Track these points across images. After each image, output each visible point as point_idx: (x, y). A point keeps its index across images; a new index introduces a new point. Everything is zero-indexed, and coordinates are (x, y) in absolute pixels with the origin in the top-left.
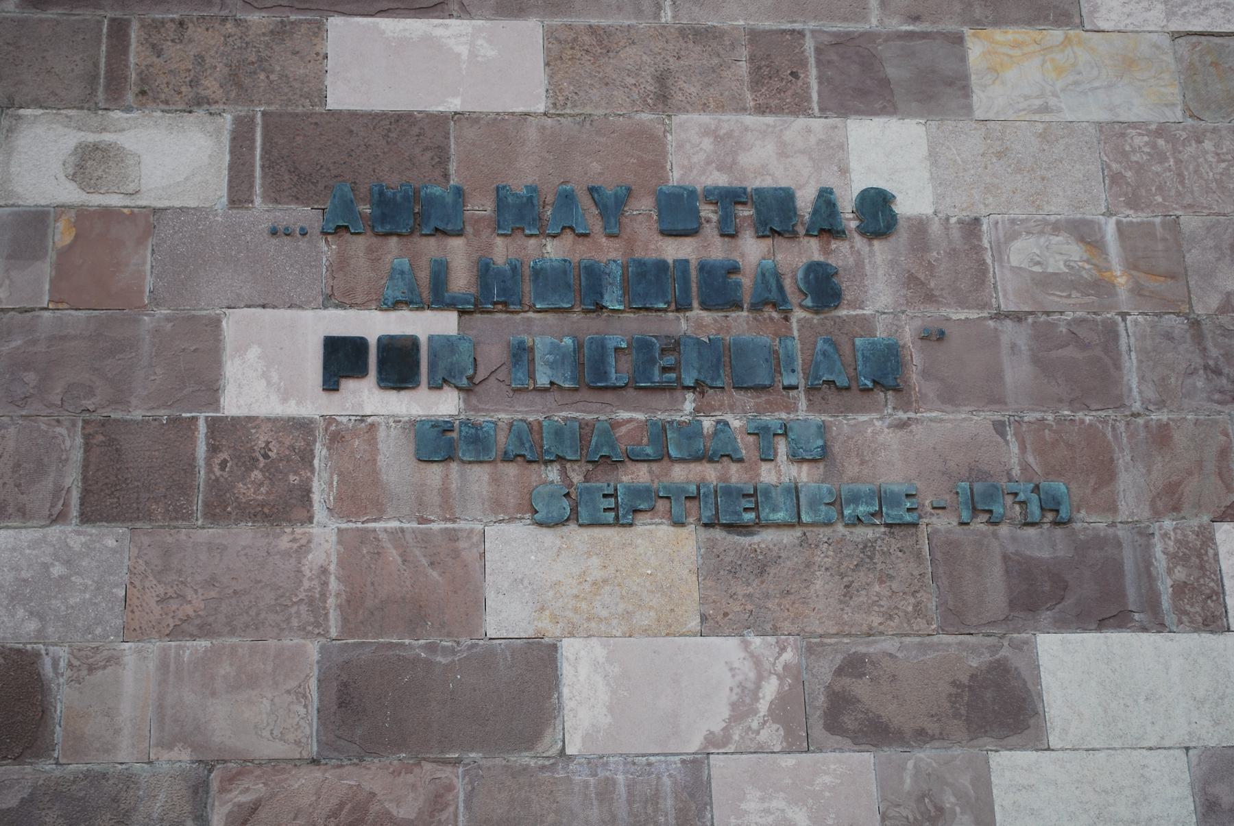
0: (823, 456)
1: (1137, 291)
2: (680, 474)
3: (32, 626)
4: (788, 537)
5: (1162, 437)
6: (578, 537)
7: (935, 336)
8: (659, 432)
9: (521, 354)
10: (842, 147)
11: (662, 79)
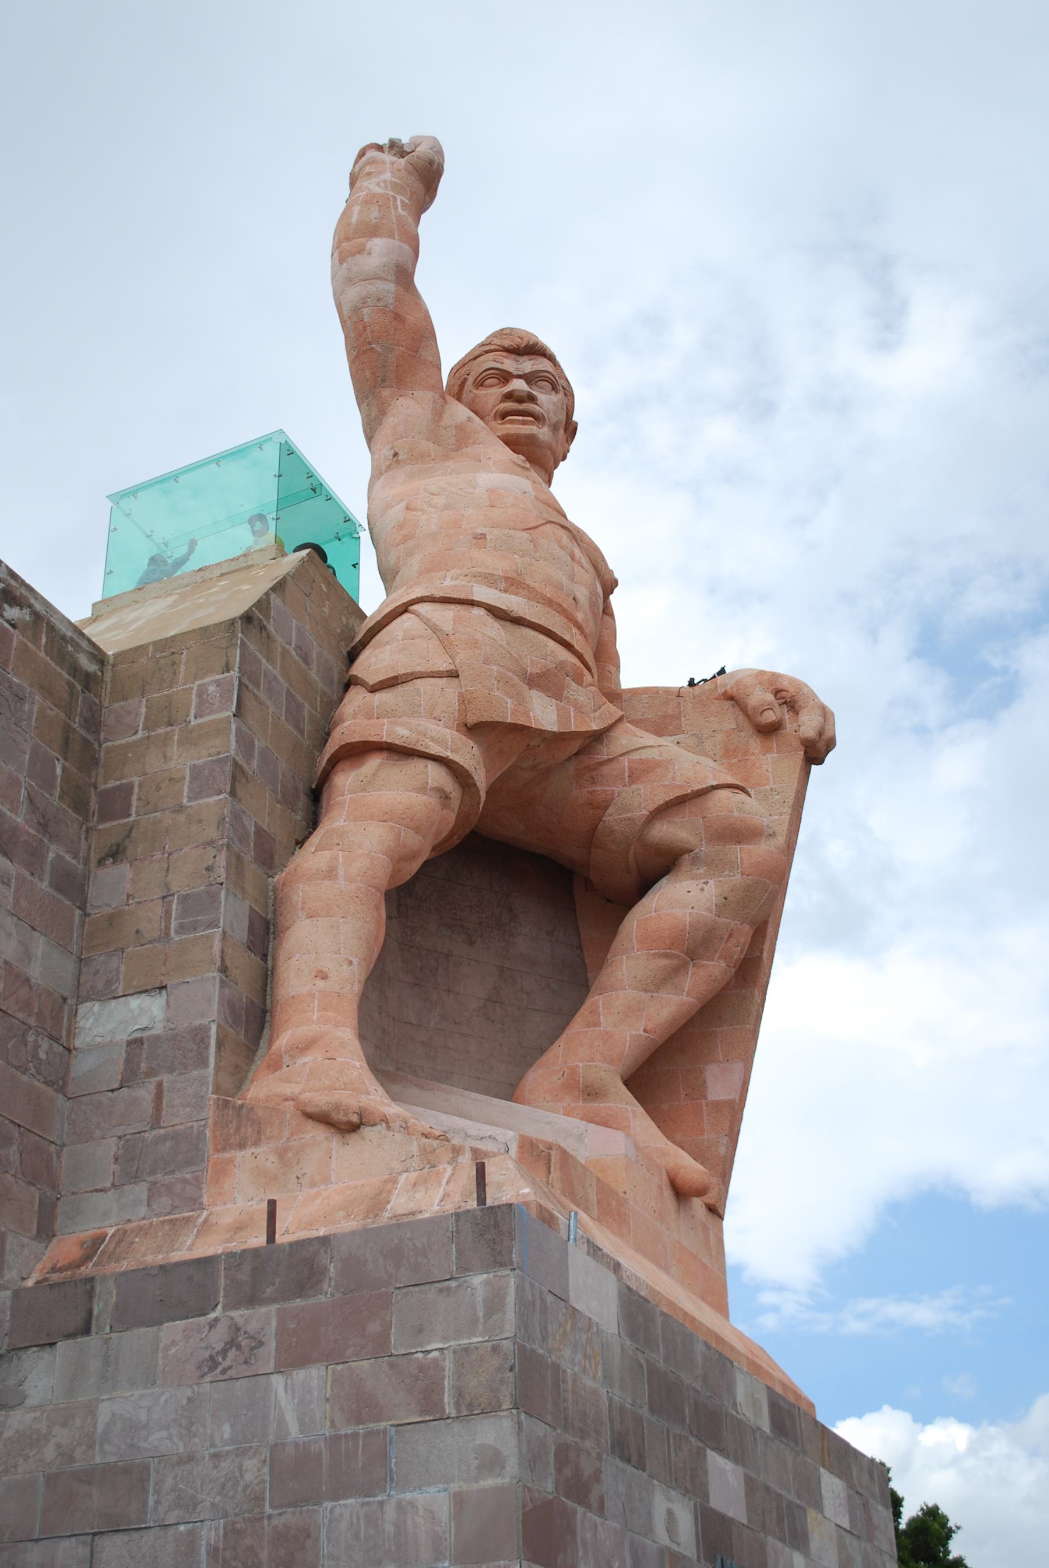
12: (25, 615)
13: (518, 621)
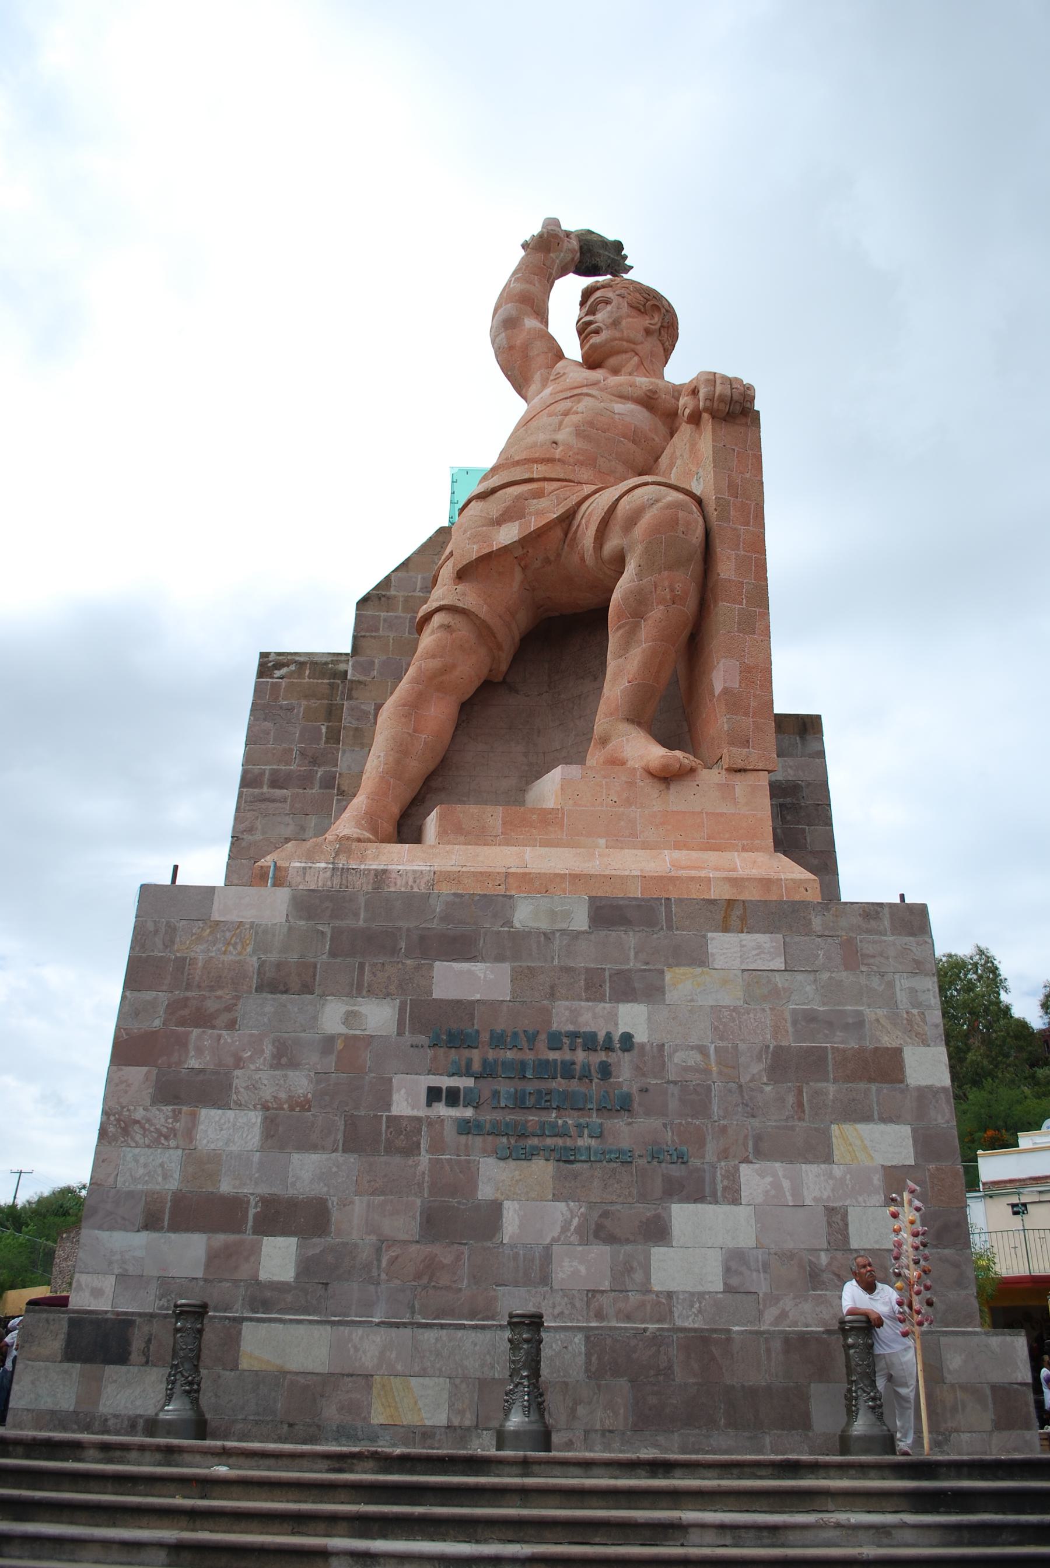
0: (600, 1136)
1: (720, 1073)
2: (549, 1141)
3: (325, 1189)
4: (586, 1166)
5: (724, 1130)
6: (512, 1164)
7: (644, 1090)
8: (543, 1125)
9: (496, 1094)
10: (616, 1015)
11: (552, 987)
12: (293, 667)
13: (494, 491)
